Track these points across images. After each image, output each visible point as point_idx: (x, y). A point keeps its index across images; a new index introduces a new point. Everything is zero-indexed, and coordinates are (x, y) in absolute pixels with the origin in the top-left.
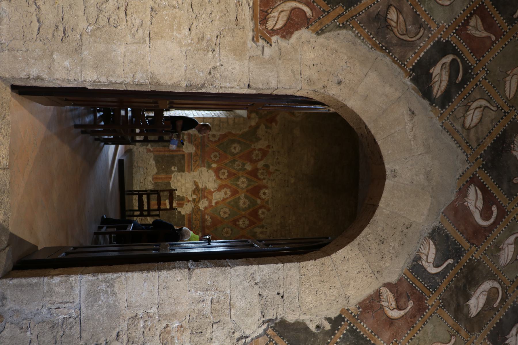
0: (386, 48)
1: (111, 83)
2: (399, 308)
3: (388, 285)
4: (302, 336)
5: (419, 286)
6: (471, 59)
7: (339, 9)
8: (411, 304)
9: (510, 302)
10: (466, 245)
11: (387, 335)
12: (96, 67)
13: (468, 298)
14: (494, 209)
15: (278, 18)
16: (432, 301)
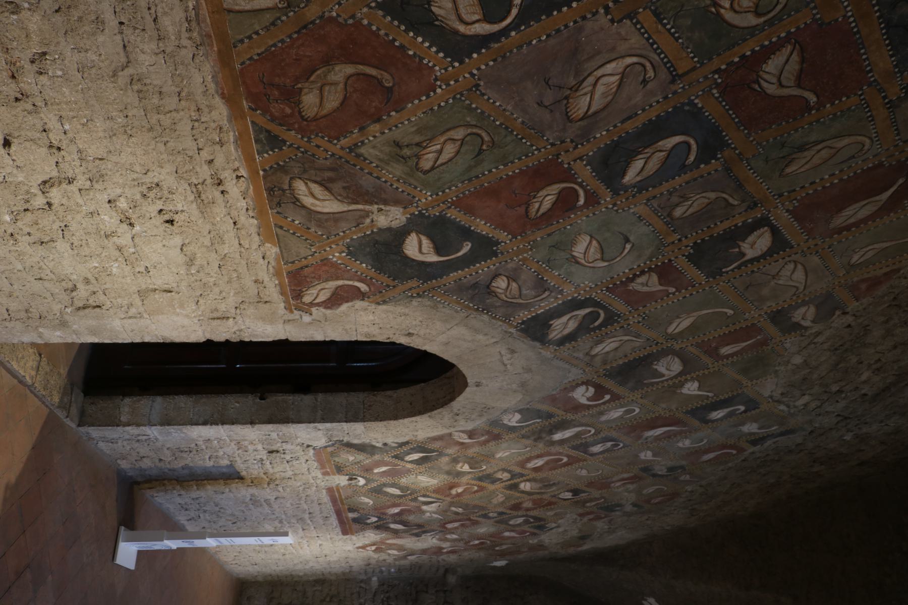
7: (413, 283)
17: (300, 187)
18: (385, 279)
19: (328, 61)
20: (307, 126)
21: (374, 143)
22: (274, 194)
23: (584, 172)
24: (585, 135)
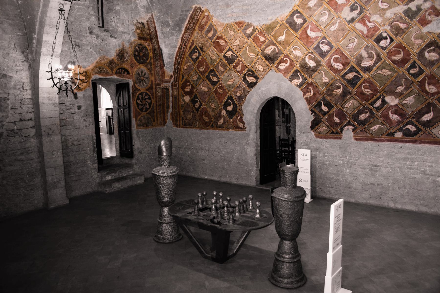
0: (245, 96)
1: (256, 164)
2: (311, 92)
3: (304, 95)
4: (315, 122)
5: (304, 85)
6: (247, 70)
7: (238, 109)
8: (310, 87)
9: (313, 51)
10: (295, 69)
11: (318, 95)
12: (253, 167)
13: (310, 67)
14: (285, 59)
15: (241, 125)
16: (310, 80)
17: (219, 124)
18: (237, 114)
19: (203, 118)
20: (210, 121)
21: (212, 114)
22: (220, 127)
23: (216, 87)
24: (210, 88)
